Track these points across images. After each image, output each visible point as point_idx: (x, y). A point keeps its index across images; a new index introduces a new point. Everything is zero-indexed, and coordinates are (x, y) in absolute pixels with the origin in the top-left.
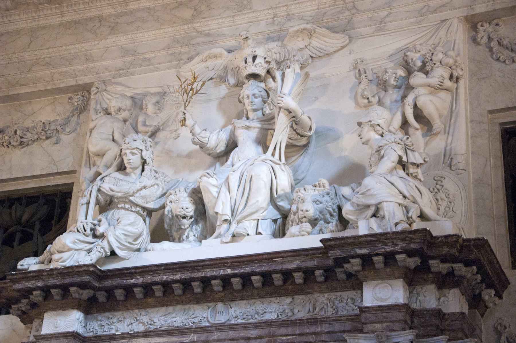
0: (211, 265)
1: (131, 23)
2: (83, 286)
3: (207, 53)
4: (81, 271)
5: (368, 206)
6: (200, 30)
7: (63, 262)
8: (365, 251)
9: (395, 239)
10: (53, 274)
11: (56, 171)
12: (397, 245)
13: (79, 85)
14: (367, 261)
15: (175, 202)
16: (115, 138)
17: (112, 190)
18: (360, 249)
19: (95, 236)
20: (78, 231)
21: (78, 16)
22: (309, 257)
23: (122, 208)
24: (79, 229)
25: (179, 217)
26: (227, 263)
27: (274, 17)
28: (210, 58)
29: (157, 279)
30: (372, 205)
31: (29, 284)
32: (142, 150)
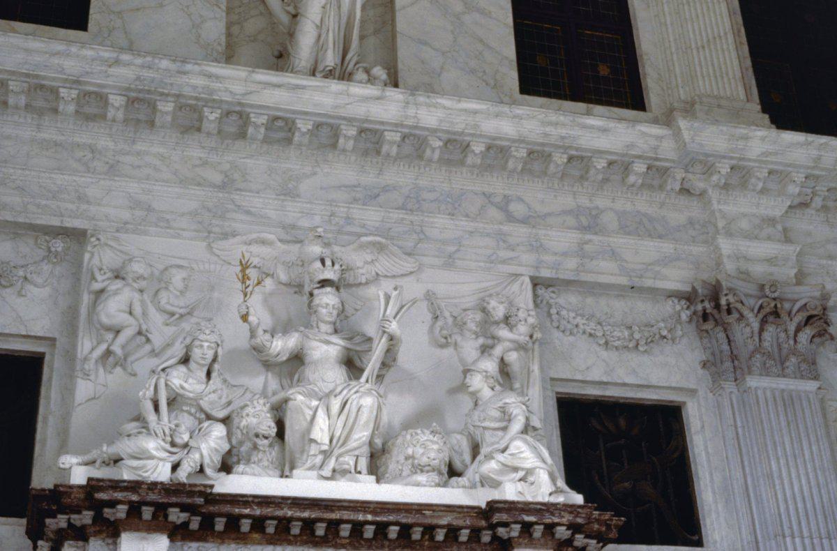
0: (350, 507)
1: (139, 167)
2: (184, 508)
3: (254, 236)
4: (194, 491)
5: (516, 469)
6: (238, 204)
7: (147, 471)
8: (532, 519)
9: (564, 511)
10: (156, 489)
11: (24, 333)
12: (563, 517)
13: (66, 228)
14: (527, 528)
15: (254, 417)
16: (135, 312)
17: (182, 388)
18: (528, 515)
19: (173, 444)
20: (156, 435)
21: (63, 138)
22: (462, 515)
23: (187, 411)
24: (158, 432)
25: (261, 436)
26: (369, 508)
27: (331, 216)
28: (256, 242)
29: (279, 513)
30: (523, 469)
31: (119, 495)
32: (218, 345)
